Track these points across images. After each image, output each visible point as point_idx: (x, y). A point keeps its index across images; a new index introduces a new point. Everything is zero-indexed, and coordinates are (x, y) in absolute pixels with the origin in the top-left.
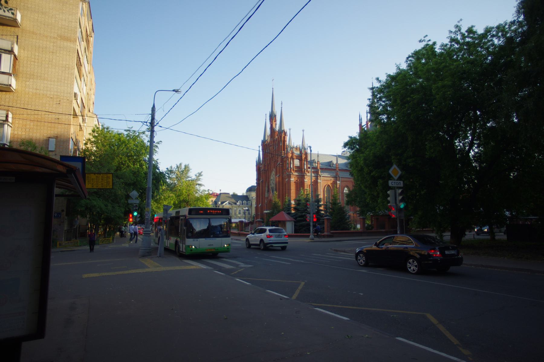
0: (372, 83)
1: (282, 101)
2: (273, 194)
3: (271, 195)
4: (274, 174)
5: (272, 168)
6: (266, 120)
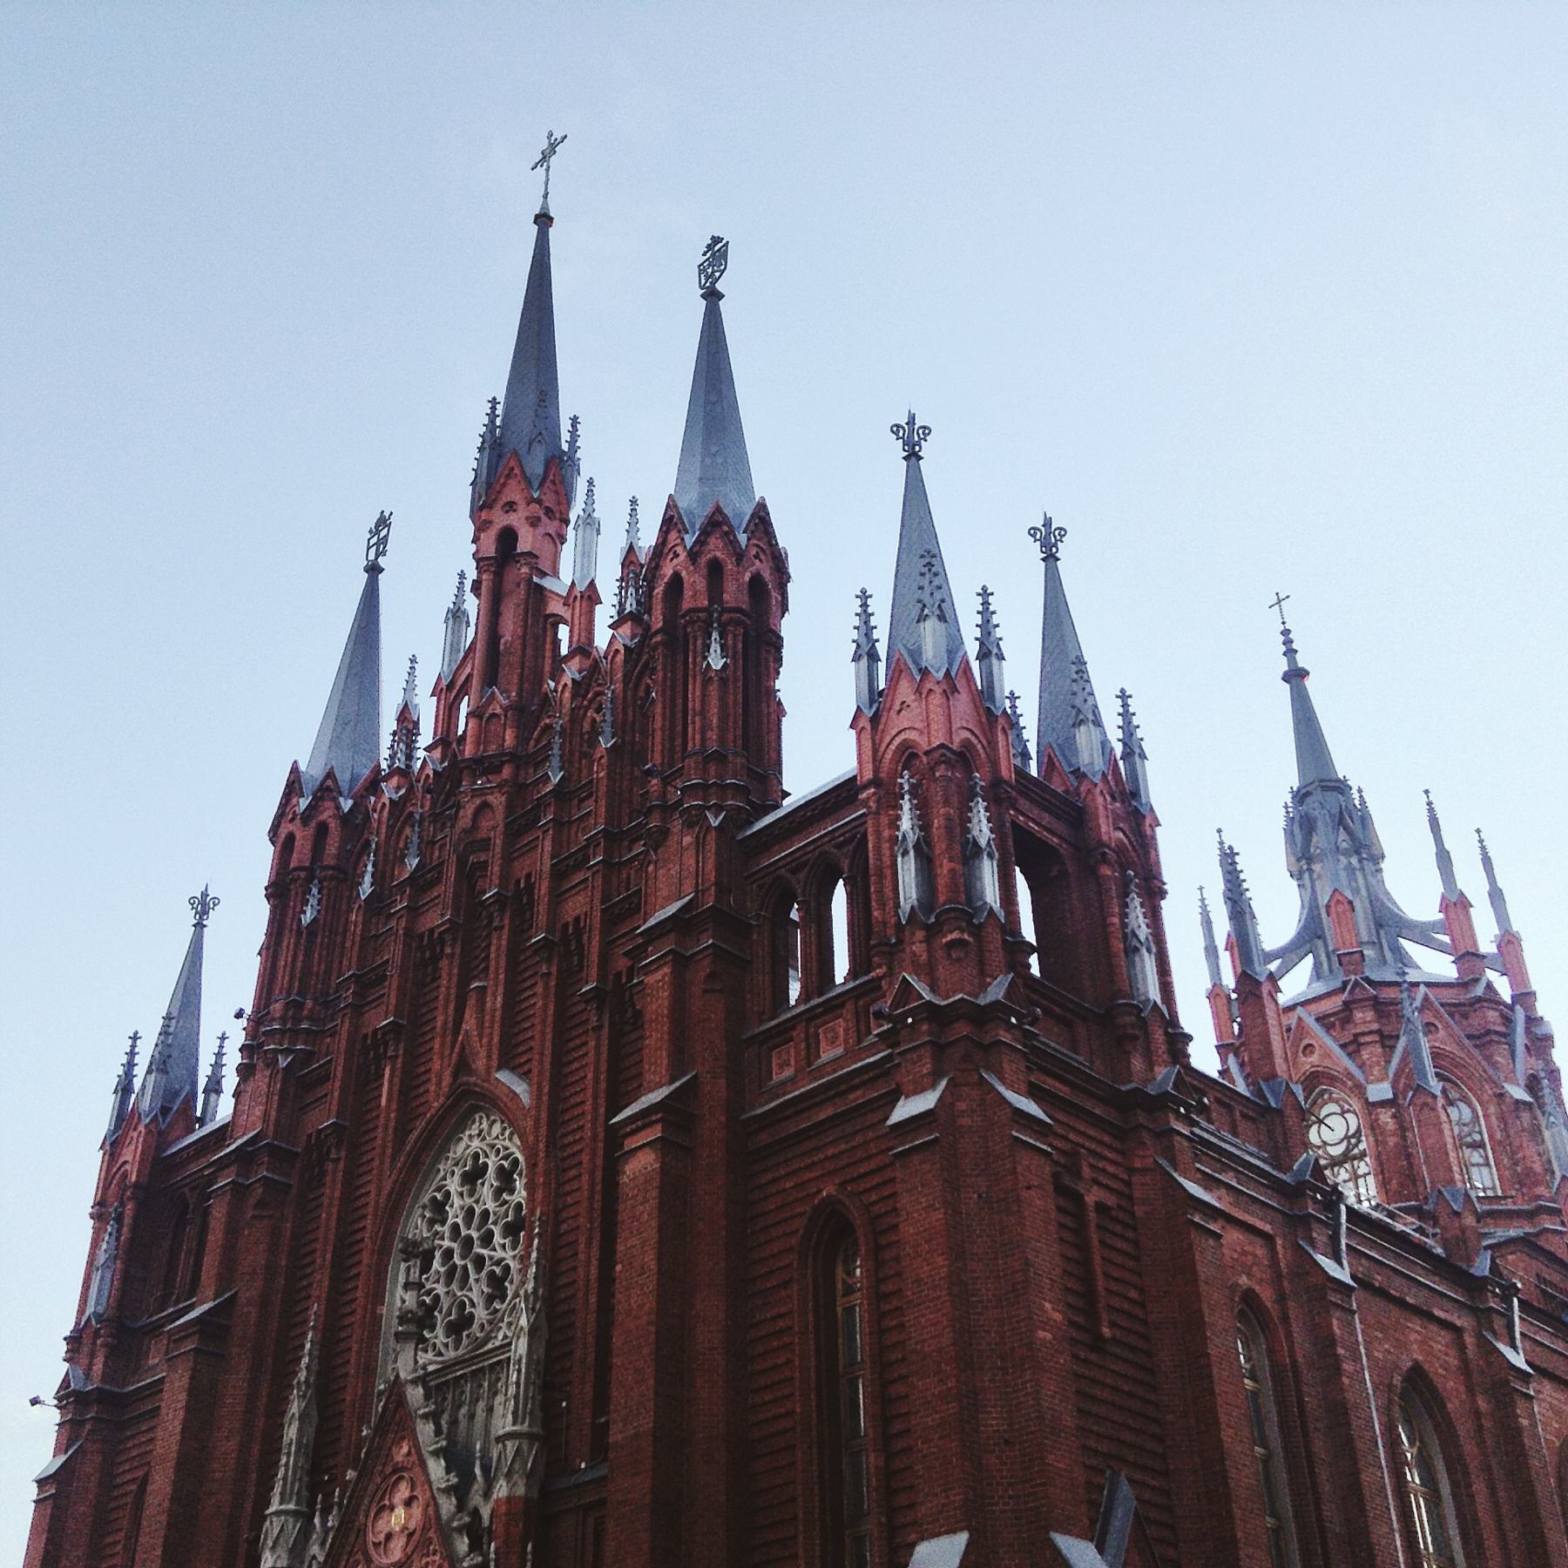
0: (1286, 632)
1: (716, 240)
2: (460, 1492)
3: (397, 1518)
4: (473, 1177)
5: (463, 1066)
6: (374, 570)
